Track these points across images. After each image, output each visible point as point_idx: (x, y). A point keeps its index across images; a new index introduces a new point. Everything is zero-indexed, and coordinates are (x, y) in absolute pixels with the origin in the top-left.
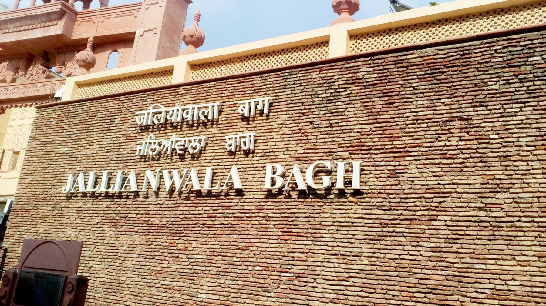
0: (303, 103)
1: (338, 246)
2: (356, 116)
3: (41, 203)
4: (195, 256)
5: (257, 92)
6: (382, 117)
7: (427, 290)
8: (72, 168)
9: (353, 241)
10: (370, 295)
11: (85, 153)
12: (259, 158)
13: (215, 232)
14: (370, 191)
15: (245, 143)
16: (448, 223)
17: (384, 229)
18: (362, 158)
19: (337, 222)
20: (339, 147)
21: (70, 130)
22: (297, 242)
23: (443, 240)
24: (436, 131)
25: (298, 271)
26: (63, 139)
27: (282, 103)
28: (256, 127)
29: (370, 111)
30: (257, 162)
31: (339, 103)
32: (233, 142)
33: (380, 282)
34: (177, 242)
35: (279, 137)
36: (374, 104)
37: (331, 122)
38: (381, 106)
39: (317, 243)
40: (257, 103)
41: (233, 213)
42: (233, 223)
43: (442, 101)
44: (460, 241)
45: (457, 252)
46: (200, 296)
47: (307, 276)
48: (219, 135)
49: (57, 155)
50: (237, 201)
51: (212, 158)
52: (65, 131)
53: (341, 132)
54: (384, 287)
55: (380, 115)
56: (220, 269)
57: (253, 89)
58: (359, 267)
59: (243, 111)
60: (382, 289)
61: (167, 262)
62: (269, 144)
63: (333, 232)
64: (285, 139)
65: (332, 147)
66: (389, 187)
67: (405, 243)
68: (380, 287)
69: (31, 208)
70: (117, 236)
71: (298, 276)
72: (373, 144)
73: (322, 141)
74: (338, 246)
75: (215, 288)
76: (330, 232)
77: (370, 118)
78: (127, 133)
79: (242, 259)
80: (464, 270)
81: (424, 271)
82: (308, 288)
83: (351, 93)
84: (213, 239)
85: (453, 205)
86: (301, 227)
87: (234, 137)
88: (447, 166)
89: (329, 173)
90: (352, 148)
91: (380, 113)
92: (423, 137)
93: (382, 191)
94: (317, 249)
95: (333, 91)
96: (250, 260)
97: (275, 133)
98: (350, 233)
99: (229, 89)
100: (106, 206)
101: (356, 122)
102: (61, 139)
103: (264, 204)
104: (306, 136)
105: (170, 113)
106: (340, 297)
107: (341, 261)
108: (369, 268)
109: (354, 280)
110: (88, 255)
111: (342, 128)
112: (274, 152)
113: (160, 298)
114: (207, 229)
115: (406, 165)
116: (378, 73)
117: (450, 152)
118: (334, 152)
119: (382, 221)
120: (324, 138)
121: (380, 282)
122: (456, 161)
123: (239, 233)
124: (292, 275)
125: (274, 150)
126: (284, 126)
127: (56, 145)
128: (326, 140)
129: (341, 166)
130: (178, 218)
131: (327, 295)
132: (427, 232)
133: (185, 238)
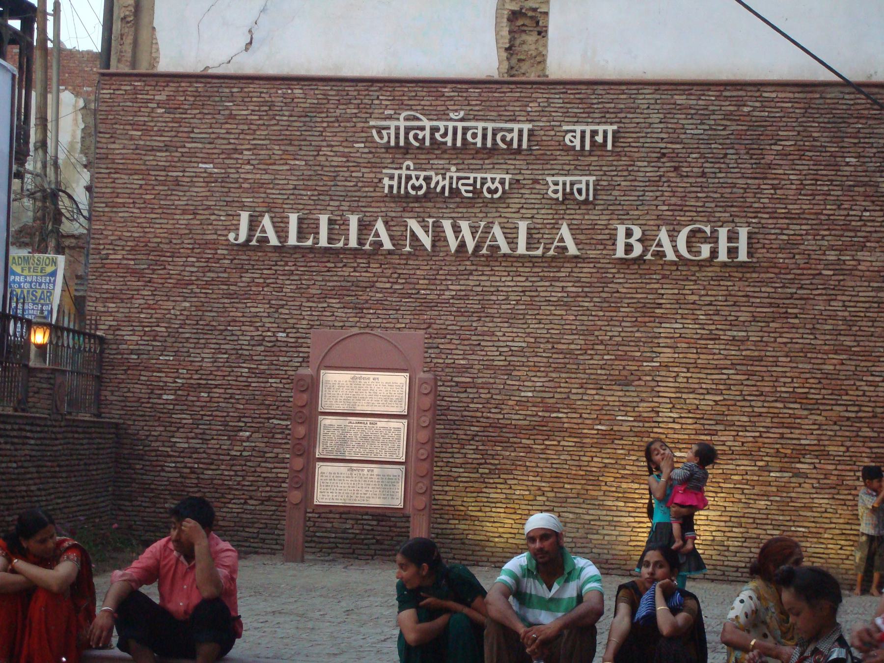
0: (662, 139)
1: (717, 329)
2: (740, 166)
3: (170, 259)
4: (508, 343)
6: (773, 171)
9: (736, 323)
10: (758, 384)
12: (600, 212)
13: (536, 312)
14: (758, 265)
15: (580, 191)
16: (847, 304)
20: (716, 206)
21: (210, 131)
22: (663, 325)
23: (840, 322)
25: (666, 360)
28: (590, 165)
29: (757, 161)
32: (560, 187)
33: (769, 369)
34: (475, 324)
35: (628, 183)
40: (594, 133)
42: (565, 299)
43: (848, 160)
44: (859, 323)
45: (855, 335)
46: (523, 394)
48: (529, 172)
49: (186, 174)
50: (569, 270)
51: (520, 206)
52: (195, 130)
56: (551, 360)
59: (572, 142)
61: (462, 352)
63: (711, 312)
65: (707, 205)
66: (781, 261)
68: (768, 374)
70: (360, 315)
71: (666, 366)
73: (693, 195)
74: (717, 329)
75: (546, 384)
77: (758, 171)
79: (584, 347)
80: (862, 354)
81: (819, 356)
84: (536, 321)
85: (853, 284)
86: (668, 306)
87: (561, 179)
89: (706, 240)
95: (707, 127)
96: (596, 347)
97: (623, 178)
99: (539, 100)
100: (326, 269)
101: (739, 175)
102: (188, 145)
103: (611, 276)
104: (669, 186)
105: (442, 131)
106: (721, 387)
107: (722, 347)
108: (756, 353)
109: (738, 367)
111: (721, 181)
113: (457, 400)
114: (524, 307)
115: (801, 235)
117: (853, 223)
119: (773, 301)
120: (697, 192)
121: (769, 369)
122: (859, 234)
123: (576, 313)
124: (658, 364)
125: (622, 203)
127: (179, 155)
128: (699, 195)
129: (723, 233)
130: (472, 290)
131: (704, 386)
133: (488, 319)
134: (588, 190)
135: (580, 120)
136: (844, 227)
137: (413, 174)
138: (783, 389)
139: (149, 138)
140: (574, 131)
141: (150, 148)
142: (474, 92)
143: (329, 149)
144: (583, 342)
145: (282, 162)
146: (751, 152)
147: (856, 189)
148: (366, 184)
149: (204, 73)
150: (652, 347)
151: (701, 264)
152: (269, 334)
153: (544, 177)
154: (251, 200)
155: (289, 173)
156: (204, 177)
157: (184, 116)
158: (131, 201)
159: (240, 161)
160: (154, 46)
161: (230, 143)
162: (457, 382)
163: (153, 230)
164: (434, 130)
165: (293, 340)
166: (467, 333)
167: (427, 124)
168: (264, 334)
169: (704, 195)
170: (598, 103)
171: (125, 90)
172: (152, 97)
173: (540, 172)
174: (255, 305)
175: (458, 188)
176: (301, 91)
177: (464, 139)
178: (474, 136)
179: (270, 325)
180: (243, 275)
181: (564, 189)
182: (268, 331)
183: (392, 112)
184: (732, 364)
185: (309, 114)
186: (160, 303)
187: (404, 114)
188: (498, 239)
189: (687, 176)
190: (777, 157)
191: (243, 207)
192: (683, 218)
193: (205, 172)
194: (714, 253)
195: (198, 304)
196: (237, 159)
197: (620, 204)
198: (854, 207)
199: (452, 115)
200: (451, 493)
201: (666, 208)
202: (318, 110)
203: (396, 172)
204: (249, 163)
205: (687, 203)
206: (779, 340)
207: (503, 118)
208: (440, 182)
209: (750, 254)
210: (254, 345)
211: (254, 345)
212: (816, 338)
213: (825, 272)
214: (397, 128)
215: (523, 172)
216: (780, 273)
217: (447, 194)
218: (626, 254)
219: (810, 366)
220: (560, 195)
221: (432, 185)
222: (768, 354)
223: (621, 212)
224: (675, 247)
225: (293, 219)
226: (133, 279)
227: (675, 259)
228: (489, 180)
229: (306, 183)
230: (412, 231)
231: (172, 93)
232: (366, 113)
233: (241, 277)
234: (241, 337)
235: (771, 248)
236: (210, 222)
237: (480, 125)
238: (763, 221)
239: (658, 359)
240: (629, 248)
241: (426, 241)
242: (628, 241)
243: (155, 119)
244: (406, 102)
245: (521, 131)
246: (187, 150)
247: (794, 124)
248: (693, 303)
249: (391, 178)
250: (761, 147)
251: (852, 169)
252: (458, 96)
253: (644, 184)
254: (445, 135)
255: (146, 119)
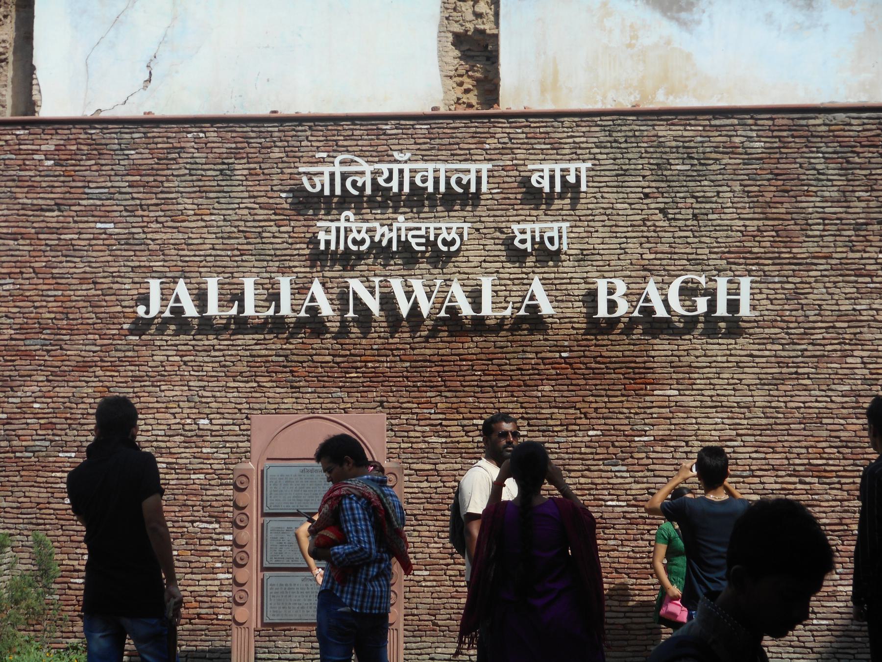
0: (644, 177)
2: (735, 205)
3: (68, 337)
5: (556, 147)
6: (774, 210)
7: (839, 444)
8: (140, 266)
9: (739, 387)
11: (169, 236)
15: (551, 240)
16: (865, 360)
17: (785, 370)
18: (746, 270)
19: (715, 362)
21: (109, 184)
22: (656, 392)
23: (859, 382)
24: (849, 236)
25: (661, 433)
26: (91, 201)
27: (607, 173)
28: (562, 209)
29: (755, 199)
30: (573, 270)
31: (706, 183)
32: (528, 236)
33: (780, 438)
36: (762, 189)
37: (696, 211)
38: (771, 194)
39: (687, 393)
41: (537, 353)
43: (857, 194)
47: (675, 438)
48: (492, 219)
52: (91, 185)
53: (712, 228)
54: (786, 444)
55: (770, 207)
57: (547, 141)
58: (750, 422)
59: (539, 183)
60: (784, 447)
62: (590, 241)
64: (618, 235)
65: (699, 251)
66: (788, 313)
67: (812, 387)
68: (780, 444)
69: (38, 347)
71: (662, 440)
72: (762, 250)
74: (718, 395)
76: (705, 376)
77: (757, 210)
78: (271, 201)
79: (565, 422)
81: (836, 421)
82: (678, 455)
83: (724, 169)
84: (504, 394)
87: (528, 227)
88: (864, 285)
90: (733, 256)
91: (771, 205)
92: (832, 244)
93: (779, 319)
94: (687, 400)
96: (578, 421)
97: (601, 224)
98: (735, 376)
104: (655, 231)
105: (386, 175)
108: (764, 421)
110: (231, 433)
111: (715, 223)
112: (602, 255)
114: (491, 378)
116: (765, 142)
118: (703, 260)
119: (780, 359)
120: (686, 237)
121: (780, 438)
124: (652, 438)
125: (601, 252)
126: (615, 212)
132: (840, 371)
134: (560, 238)
135: (547, 157)
136: (858, 272)
138: (797, 461)
139: (35, 195)
140: (542, 171)
141: (39, 207)
142: (421, 129)
143: (252, 200)
144: (563, 417)
145: (195, 218)
146: (746, 189)
147: (870, 227)
148: (298, 240)
149: (96, 117)
150: (643, 419)
151: (691, 323)
152: (189, 421)
153: (508, 225)
154: (161, 263)
155: (205, 230)
156: (104, 239)
157: (77, 168)
158: (18, 270)
159: (145, 219)
160: (35, 87)
161: (133, 199)
162: (416, 470)
163: (44, 304)
164: (377, 173)
165: (218, 428)
166: (425, 411)
167: (368, 168)
168: (183, 421)
169: (696, 240)
170: (568, 137)
171: (6, 141)
172: (38, 147)
173: (503, 219)
174: (172, 388)
175: (407, 240)
176: (215, 134)
177: (412, 183)
178: (424, 180)
179: (189, 411)
180: (154, 353)
181: (533, 238)
182: (189, 418)
183: (324, 155)
184: (738, 435)
185: (226, 161)
186: (57, 389)
187: (341, 157)
188: (458, 298)
189: (675, 219)
190: (776, 194)
191: (152, 272)
192: (673, 268)
193: (105, 233)
194: (712, 305)
195: (101, 389)
196: (142, 216)
197: (598, 254)
198: (868, 249)
199: (396, 154)
200: (415, 600)
201: (653, 256)
202: (239, 156)
203: (333, 225)
204: (158, 222)
205: (677, 250)
206: (790, 405)
207: (455, 158)
208: (384, 234)
209: (753, 308)
210: (170, 436)
211: (170, 436)
212: (832, 401)
213: (838, 325)
214: (332, 175)
215: (483, 219)
216: (788, 328)
217: (394, 248)
218: (609, 312)
219: (825, 433)
220: (528, 246)
221: (377, 239)
222: (778, 421)
223: (601, 263)
224: (666, 302)
225: (212, 286)
226: (23, 362)
227: (666, 315)
228: (444, 230)
229: (225, 241)
230: (355, 293)
231: (62, 142)
232: (294, 157)
233: (153, 355)
234: (155, 427)
235: (776, 299)
236: (112, 291)
237: (431, 166)
238: (766, 268)
239: (652, 432)
240: (612, 306)
241: (374, 304)
242: (611, 297)
243: (43, 173)
244: (340, 143)
245: (478, 171)
246: (82, 208)
247: (796, 155)
248: (690, 366)
249: (328, 231)
250: (758, 183)
251: (863, 204)
252: (403, 134)
253: (625, 229)
254: (389, 179)
255: (32, 173)
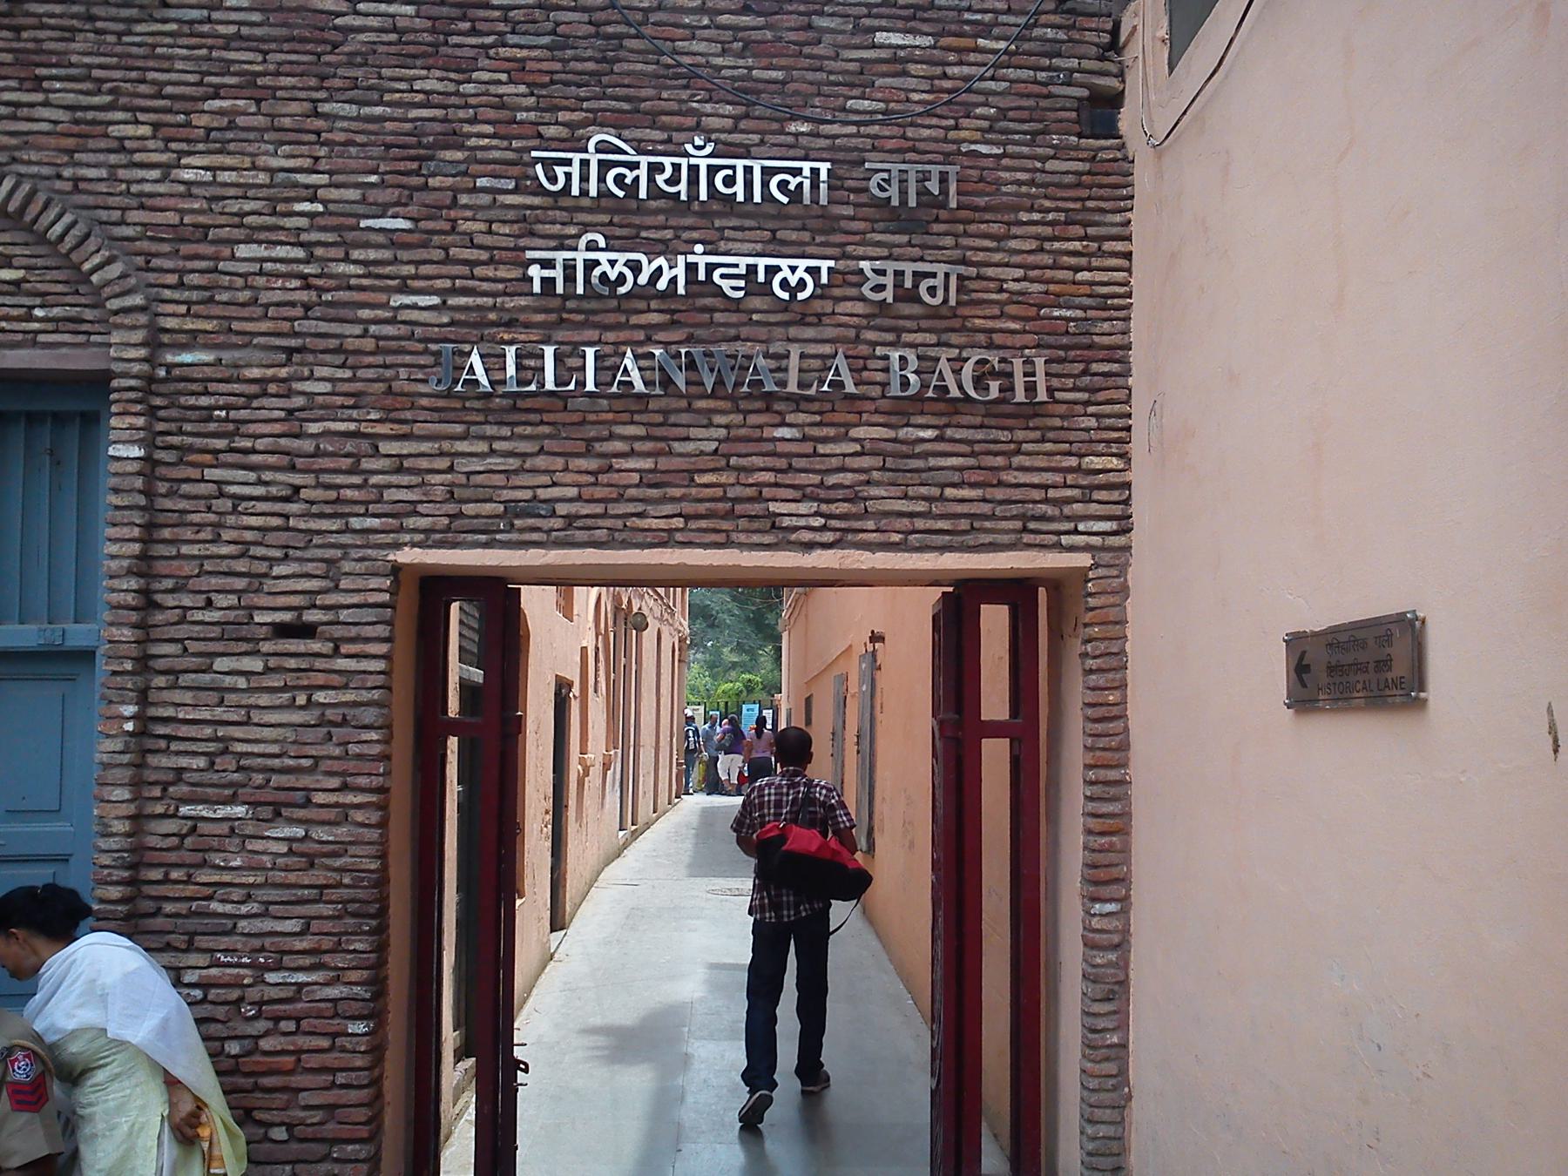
32: (889, 280)
87: (891, 266)
134: (946, 289)
137: (603, 257)
214: (585, 164)
220: (888, 295)
